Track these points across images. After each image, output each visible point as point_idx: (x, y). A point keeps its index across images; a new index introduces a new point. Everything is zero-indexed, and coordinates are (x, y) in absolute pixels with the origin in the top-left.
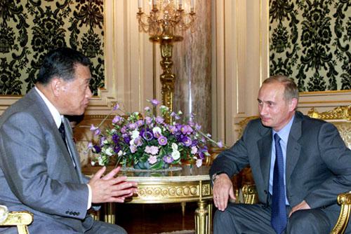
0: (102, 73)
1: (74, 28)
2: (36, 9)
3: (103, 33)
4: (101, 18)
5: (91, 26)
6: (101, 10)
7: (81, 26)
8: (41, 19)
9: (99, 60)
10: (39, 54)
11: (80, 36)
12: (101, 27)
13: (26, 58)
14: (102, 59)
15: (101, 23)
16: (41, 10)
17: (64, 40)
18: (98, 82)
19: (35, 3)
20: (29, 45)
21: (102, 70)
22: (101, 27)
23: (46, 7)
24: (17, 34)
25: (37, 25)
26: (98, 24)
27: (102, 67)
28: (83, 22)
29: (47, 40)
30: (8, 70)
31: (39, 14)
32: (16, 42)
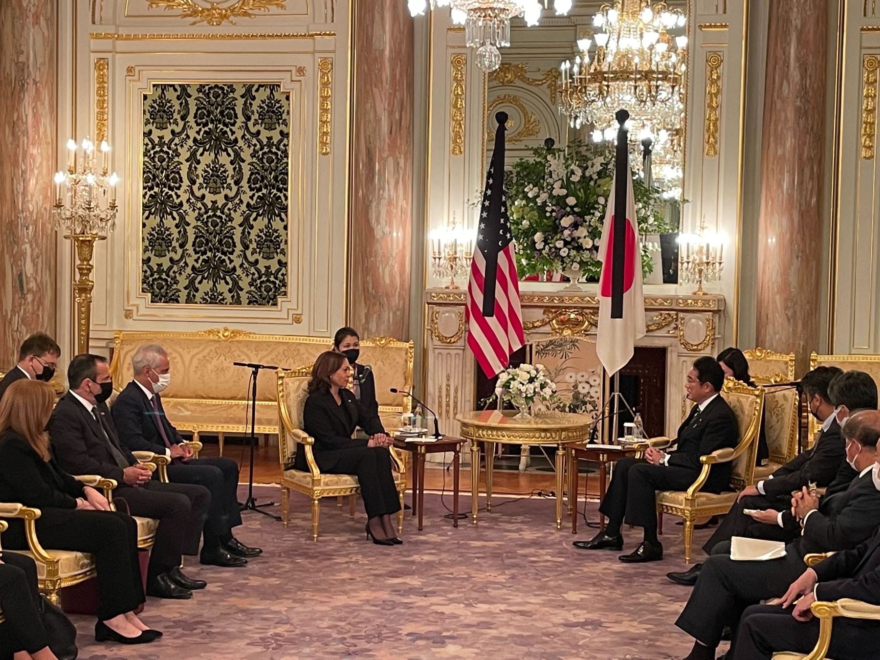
0: (284, 279)
1: (246, 223)
2: (199, 205)
3: (286, 228)
4: (285, 209)
5: (269, 220)
6: (283, 199)
7: (255, 219)
8: (205, 216)
9: (280, 262)
10: (202, 258)
11: (254, 233)
12: (282, 220)
13: (185, 263)
14: (284, 261)
15: (283, 215)
16: (204, 205)
17: (233, 239)
18: (277, 289)
19: (198, 198)
20: (189, 246)
21: (283, 275)
22: (282, 220)
23: (212, 201)
24: (176, 235)
25: (199, 223)
26: (279, 215)
27: (283, 271)
28: (258, 215)
29: (211, 241)
30: (164, 276)
31: (203, 210)
32: (174, 243)
